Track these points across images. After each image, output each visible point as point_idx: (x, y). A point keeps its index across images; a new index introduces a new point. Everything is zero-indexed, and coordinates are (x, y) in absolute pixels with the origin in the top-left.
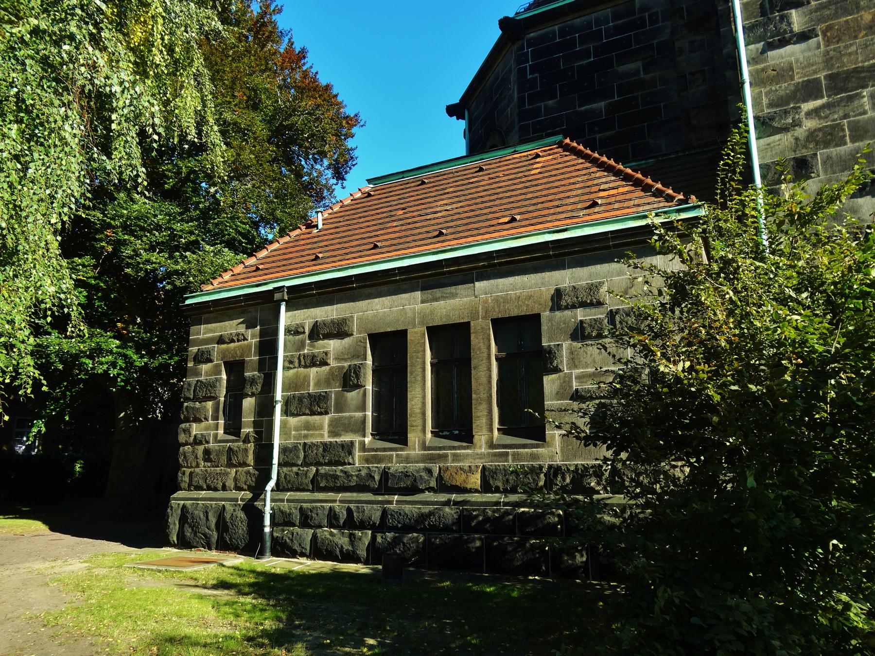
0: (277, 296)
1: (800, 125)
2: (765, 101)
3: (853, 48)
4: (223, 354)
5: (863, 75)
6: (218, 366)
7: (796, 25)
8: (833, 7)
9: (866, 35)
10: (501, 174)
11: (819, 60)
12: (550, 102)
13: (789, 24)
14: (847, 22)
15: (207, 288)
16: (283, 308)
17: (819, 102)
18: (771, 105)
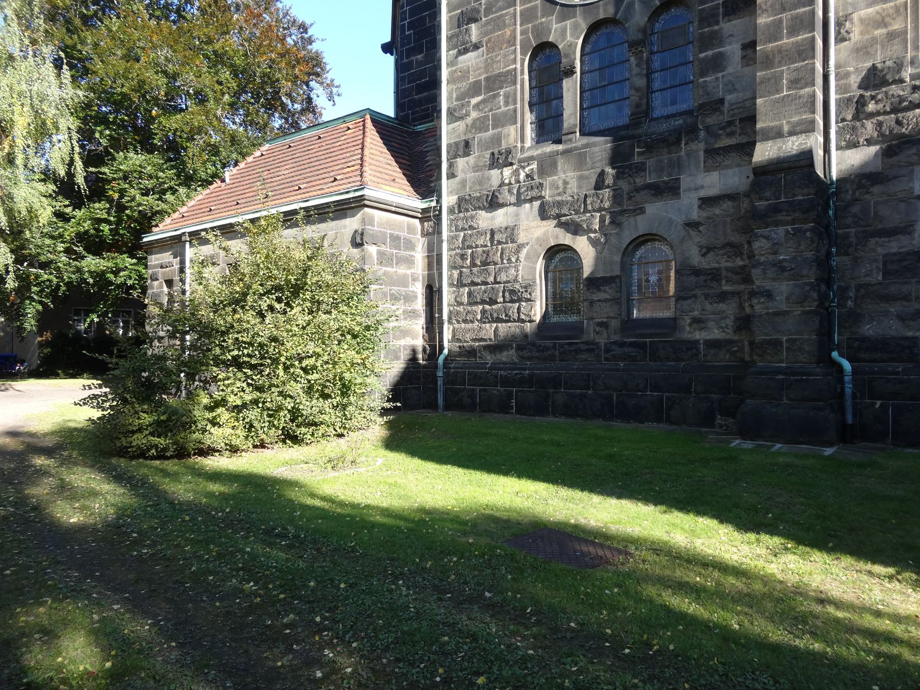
0: (183, 238)
1: (469, 115)
2: (454, 96)
3: (499, 58)
4: (163, 274)
5: (502, 78)
6: (161, 282)
7: (473, 36)
8: (492, 24)
9: (506, 48)
10: (324, 144)
11: (482, 65)
12: (419, 57)
13: (470, 36)
14: (498, 36)
15: (154, 229)
16: (187, 245)
17: (479, 98)
18: (457, 99)
